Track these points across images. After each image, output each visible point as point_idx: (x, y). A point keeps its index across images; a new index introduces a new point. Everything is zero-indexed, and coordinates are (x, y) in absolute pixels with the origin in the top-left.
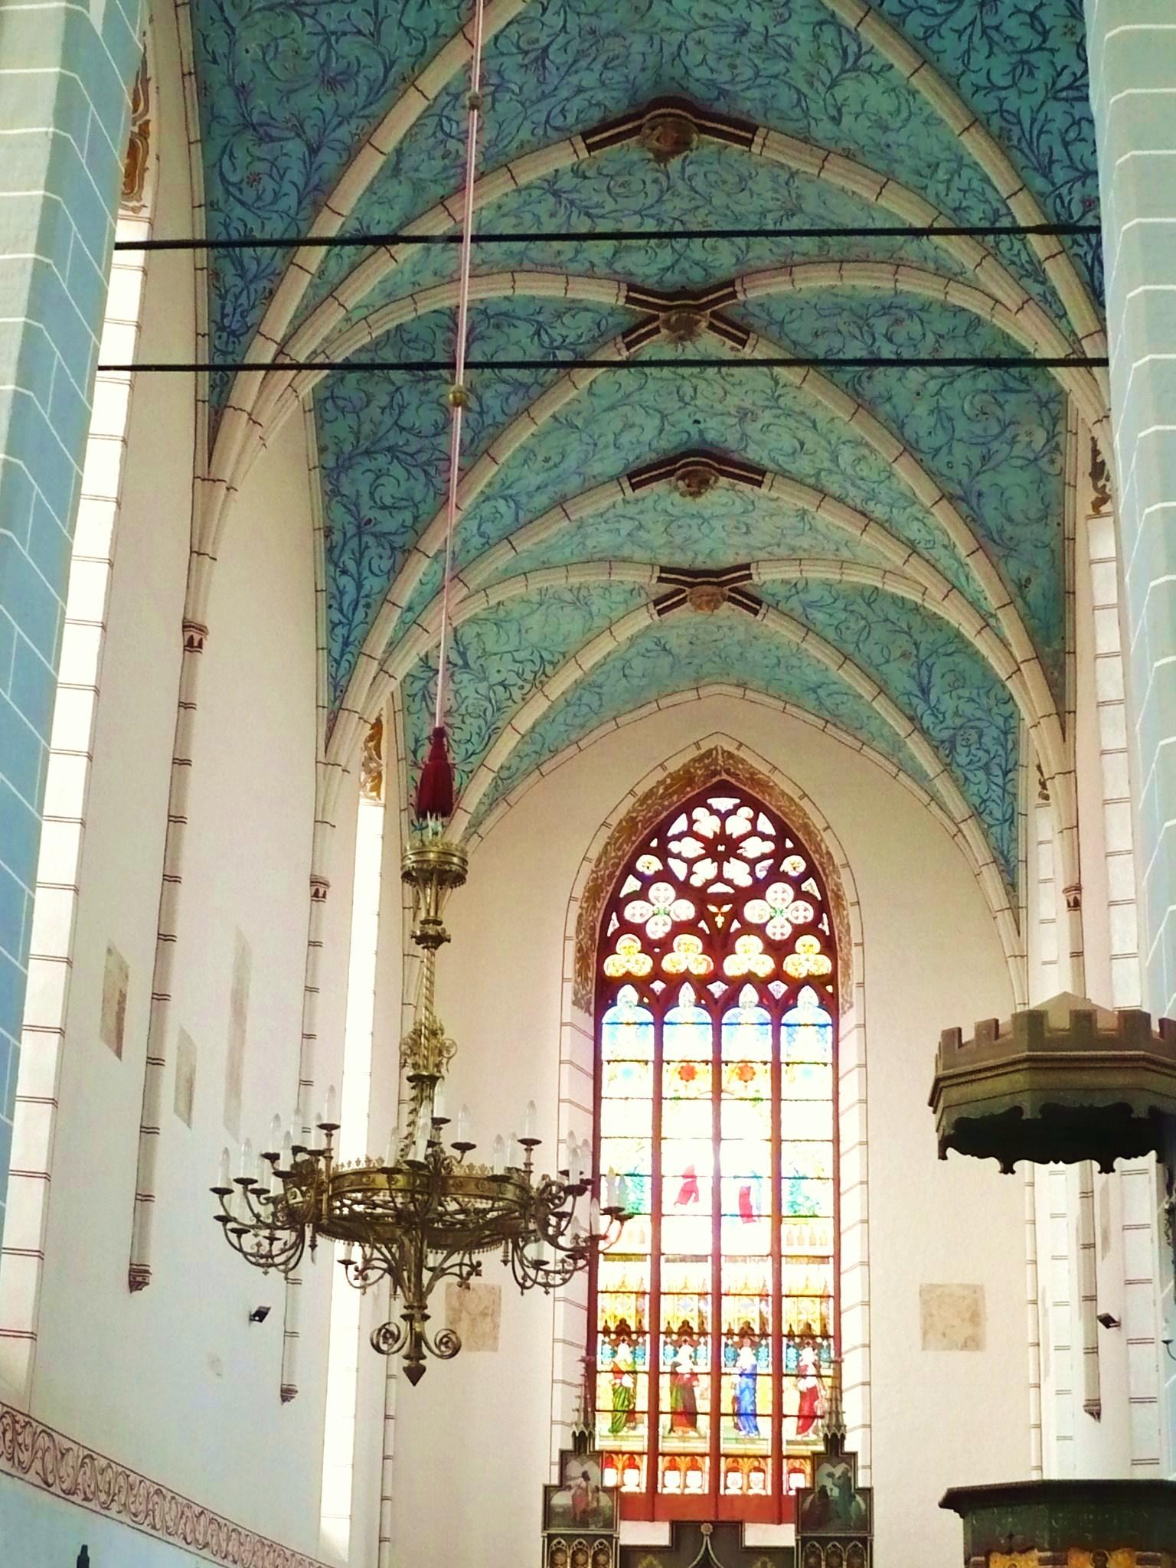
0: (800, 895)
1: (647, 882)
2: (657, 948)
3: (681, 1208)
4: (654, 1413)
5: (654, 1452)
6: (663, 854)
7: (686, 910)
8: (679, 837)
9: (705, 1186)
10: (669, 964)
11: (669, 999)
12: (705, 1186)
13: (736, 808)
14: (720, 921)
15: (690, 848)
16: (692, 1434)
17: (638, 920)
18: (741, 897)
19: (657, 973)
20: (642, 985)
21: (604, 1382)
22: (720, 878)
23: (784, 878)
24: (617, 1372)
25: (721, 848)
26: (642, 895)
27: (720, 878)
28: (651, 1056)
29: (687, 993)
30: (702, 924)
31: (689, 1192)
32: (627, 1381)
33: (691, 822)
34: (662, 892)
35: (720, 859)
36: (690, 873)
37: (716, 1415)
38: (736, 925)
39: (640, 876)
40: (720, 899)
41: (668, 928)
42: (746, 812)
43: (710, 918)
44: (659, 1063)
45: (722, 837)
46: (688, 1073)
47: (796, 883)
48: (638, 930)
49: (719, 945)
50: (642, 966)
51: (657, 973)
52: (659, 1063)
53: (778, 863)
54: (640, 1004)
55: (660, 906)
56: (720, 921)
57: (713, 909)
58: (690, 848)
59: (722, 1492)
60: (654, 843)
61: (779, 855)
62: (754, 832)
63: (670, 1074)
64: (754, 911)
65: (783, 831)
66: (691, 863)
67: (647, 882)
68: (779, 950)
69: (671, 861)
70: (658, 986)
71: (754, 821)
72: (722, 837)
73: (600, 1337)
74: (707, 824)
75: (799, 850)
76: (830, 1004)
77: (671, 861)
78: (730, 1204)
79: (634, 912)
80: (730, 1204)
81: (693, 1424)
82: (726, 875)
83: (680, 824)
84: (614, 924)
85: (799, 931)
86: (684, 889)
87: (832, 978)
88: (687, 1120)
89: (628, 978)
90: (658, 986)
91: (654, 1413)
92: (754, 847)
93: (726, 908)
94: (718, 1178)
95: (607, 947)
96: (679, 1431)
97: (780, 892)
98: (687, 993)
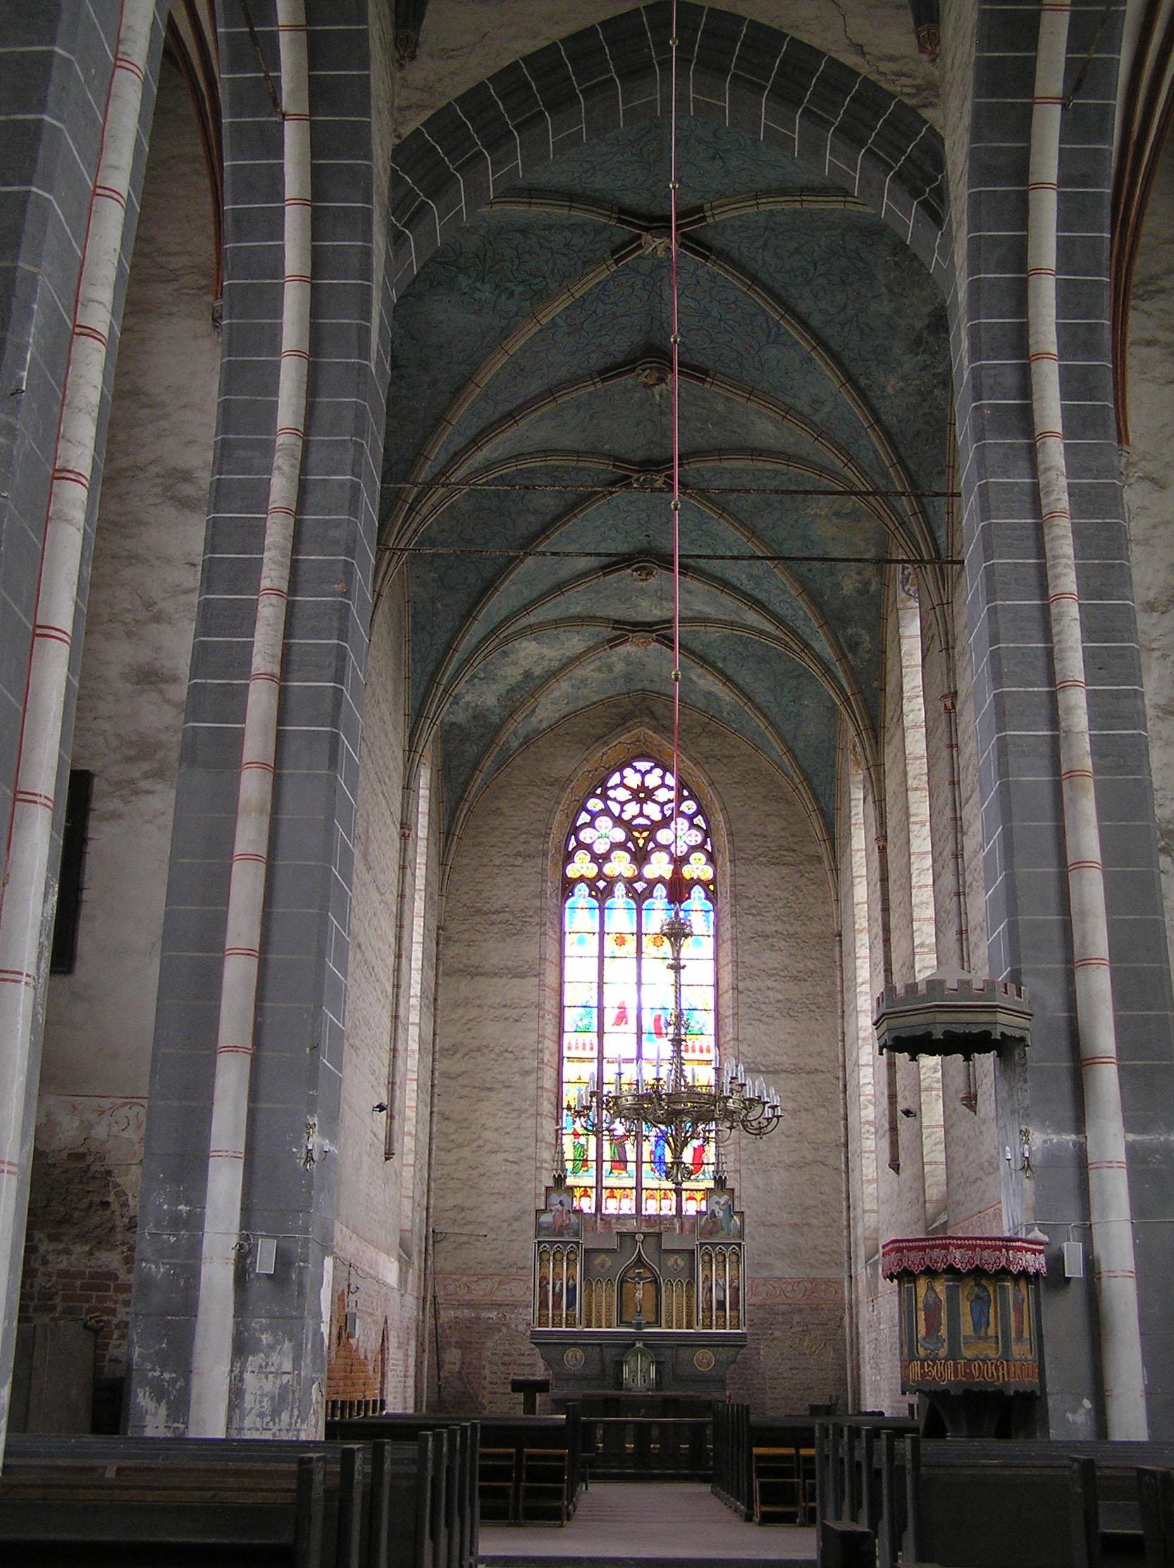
0: (693, 826)
1: (594, 816)
2: (600, 859)
3: (617, 1028)
4: (599, 1160)
5: (599, 1186)
6: (605, 797)
7: (619, 835)
8: (614, 787)
9: (632, 1014)
10: (609, 869)
11: (608, 892)
12: (632, 1014)
13: (652, 768)
14: (641, 842)
15: (623, 795)
16: (624, 1174)
17: (588, 841)
18: (654, 827)
19: (600, 875)
20: (591, 884)
21: (568, 1141)
22: (641, 814)
23: (682, 814)
24: (576, 1135)
25: (643, 795)
26: (591, 824)
27: (641, 814)
28: (597, 929)
29: (620, 889)
30: (630, 844)
31: (621, 1018)
32: (582, 1140)
33: (623, 777)
34: (604, 822)
35: (641, 802)
36: (622, 811)
37: (639, 1162)
38: (651, 845)
39: (589, 812)
40: (643, 828)
41: (608, 847)
42: (658, 772)
43: (635, 841)
44: (602, 934)
45: (643, 788)
46: (621, 941)
47: (690, 818)
48: (588, 847)
49: (640, 857)
50: (591, 871)
51: (600, 875)
52: (602, 934)
53: (679, 806)
54: (590, 895)
55: (603, 832)
56: (641, 842)
57: (637, 834)
58: (623, 795)
59: (644, 1212)
60: (599, 791)
61: (680, 799)
62: (663, 785)
63: (609, 941)
64: (663, 836)
65: (682, 785)
66: (622, 804)
67: (594, 816)
68: (679, 862)
69: (609, 803)
70: (601, 884)
71: (663, 778)
72: (643, 788)
73: (565, 1111)
74: (633, 779)
75: (692, 797)
76: (711, 897)
77: (609, 803)
78: (648, 1025)
79: (586, 835)
80: (648, 1025)
81: (625, 1169)
82: (645, 812)
83: (616, 779)
84: (573, 843)
85: (693, 849)
86: (618, 821)
87: (713, 881)
88: (620, 972)
89: (582, 879)
90: (601, 884)
91: (599, 1160)
92: (663, 795)
93: (645, 834)
94: (640, 1009)
95: (569, 858)
96: (616, 1172)
97: (682, 823)
98: (620, 889)
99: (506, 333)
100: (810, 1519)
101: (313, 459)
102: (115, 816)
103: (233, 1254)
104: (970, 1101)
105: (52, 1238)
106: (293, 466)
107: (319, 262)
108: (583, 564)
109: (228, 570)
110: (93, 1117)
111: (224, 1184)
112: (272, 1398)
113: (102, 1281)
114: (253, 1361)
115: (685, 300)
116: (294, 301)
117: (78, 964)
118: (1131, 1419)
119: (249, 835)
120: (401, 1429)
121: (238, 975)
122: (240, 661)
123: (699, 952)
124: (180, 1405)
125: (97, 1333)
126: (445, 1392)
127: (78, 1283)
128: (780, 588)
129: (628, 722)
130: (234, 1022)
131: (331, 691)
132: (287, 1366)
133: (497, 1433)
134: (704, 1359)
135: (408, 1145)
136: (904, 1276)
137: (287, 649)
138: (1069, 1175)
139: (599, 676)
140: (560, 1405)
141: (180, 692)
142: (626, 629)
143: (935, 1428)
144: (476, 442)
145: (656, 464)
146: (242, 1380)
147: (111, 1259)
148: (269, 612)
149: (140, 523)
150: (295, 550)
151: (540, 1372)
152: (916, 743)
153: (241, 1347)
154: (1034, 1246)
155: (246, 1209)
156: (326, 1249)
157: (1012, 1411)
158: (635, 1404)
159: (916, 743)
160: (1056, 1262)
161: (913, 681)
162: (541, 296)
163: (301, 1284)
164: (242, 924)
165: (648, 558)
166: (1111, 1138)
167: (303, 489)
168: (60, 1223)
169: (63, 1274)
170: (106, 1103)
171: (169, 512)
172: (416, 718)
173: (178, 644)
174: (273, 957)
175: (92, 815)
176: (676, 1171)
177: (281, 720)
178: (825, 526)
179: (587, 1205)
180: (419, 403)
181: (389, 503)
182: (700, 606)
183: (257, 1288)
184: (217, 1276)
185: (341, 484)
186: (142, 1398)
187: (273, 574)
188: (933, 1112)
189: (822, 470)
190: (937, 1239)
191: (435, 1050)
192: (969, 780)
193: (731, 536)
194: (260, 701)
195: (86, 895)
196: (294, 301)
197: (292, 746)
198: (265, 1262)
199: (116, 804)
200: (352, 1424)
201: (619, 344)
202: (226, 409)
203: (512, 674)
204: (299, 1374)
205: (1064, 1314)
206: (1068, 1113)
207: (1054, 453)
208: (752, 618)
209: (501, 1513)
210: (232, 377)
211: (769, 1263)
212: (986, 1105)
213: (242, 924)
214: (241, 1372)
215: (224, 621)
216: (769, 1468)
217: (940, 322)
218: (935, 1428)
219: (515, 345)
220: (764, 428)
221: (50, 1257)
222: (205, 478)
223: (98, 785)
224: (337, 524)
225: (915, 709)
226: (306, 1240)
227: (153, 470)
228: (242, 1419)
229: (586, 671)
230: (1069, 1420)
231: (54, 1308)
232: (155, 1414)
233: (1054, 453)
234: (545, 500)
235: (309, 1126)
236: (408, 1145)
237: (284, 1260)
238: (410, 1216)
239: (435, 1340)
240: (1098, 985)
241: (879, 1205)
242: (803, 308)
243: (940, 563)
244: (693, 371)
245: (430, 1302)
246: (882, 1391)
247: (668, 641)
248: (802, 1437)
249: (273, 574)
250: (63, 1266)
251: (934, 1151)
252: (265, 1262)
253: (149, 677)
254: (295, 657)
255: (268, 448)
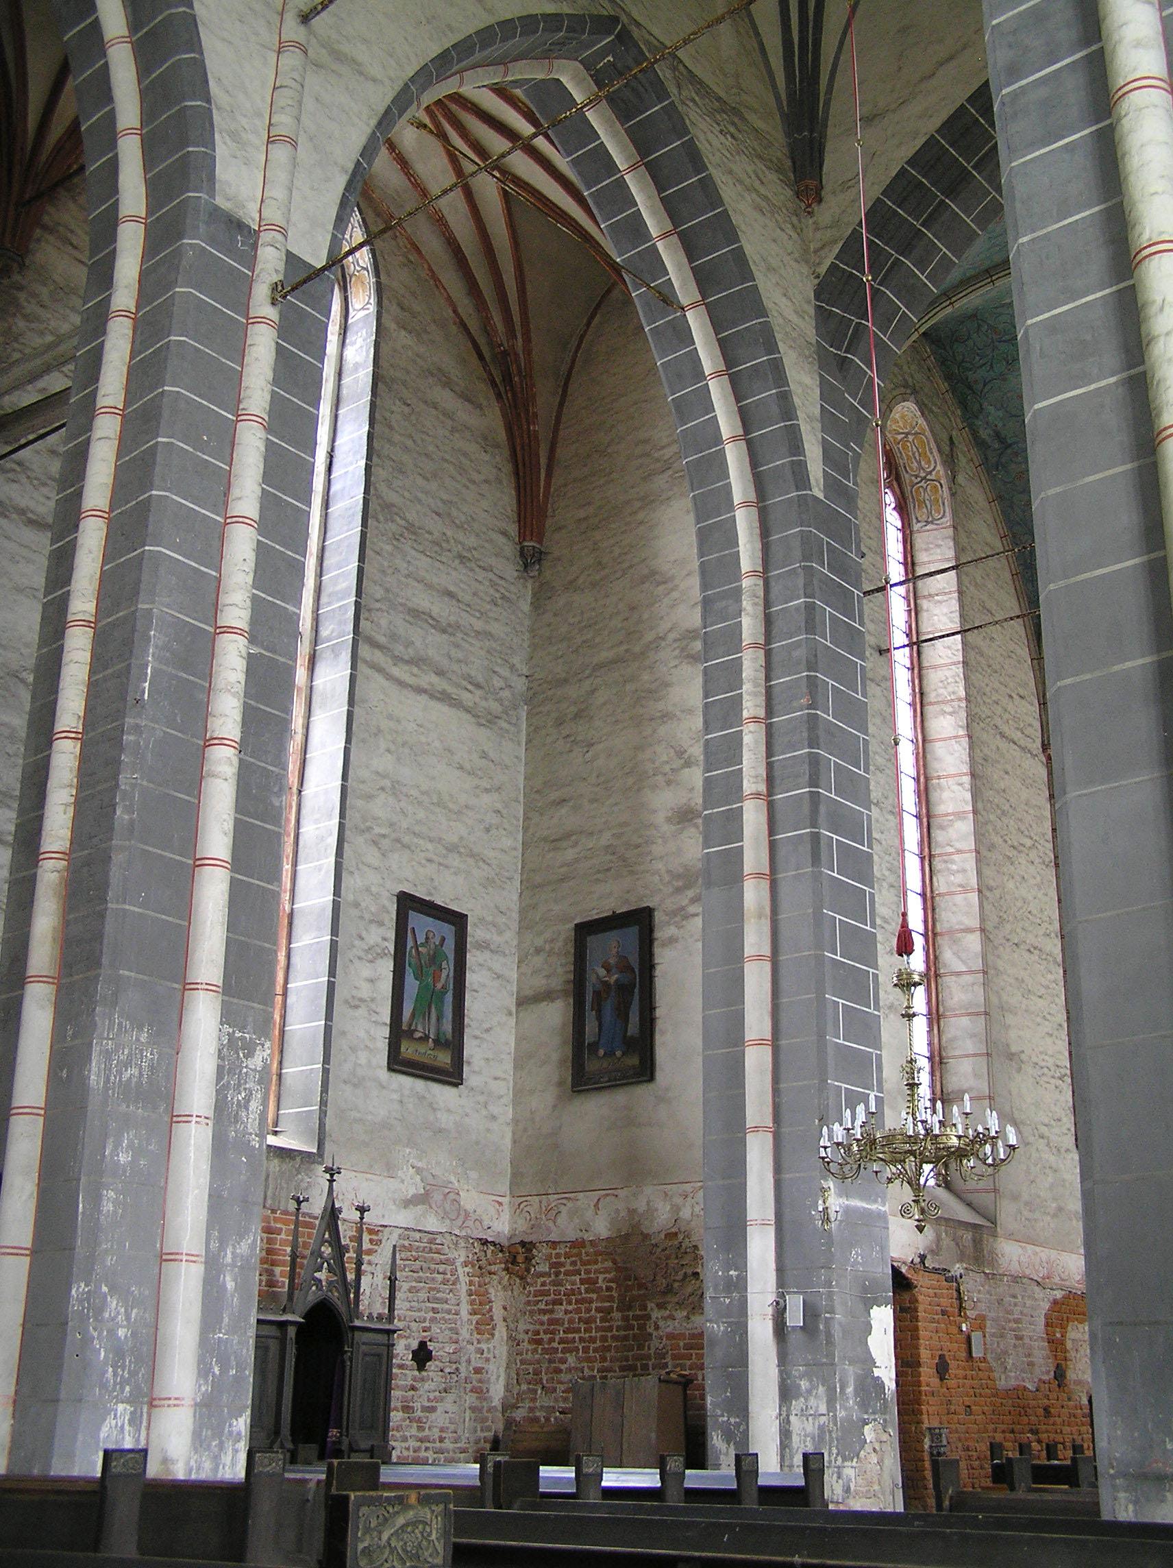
101: (776, 589)
102: (672, 940)
103: (770, 1311)
105: (661, 1306)
106: (756, 604)
110: (678, 1200)
111: (761, 1248)
112: (813, 1438)
114: (797, 1405)
117: (659, 1075)
119: (755, 939)
121: (757, 1062)
127: (681, 1344)
130: (757, 1108)
131: (807, 796)
132: (823, 1409)
137: (770, 766)
146: (789, 1422)
149: (667, 685)
150: (768, 678)
153: (787, 1393)
155: (780, 1270)
163: (829, 1335)
167: (768, 620)
168: (664, 1293)
169: (671, 1336)
170: (687, 1187)
174: (783, 1042)
175: (656, 943)
177: (772, 831)
183: (794, 1339)
184: (761, 1330)
185: (797, 608)
195: (658, 1013)
197: (782, 852)
199: (671, 931)
204: (835, 1416)
210: (704, 537)
214: (788, 1416)
221: (661, 1323)
223: (659, 917)
224: (797, 645)
226: (830, 1295)
227: (671, 636)
228: (792, 1458)
231: (666, 1365)
232: (727, 1454)
235: (823, 1190)
237: (811, 1312)
250: (669, 1330)
254: (777, 773)
255: (737, 594)
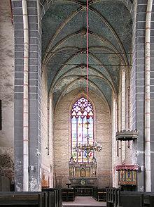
25: (83, 103)
49: (83, 112)
74: (81, 101)
88: (80, 129)
99: (60, 25)
100: (105, 201)
101: (31, 48)
104: (129, 147)
107: (28, 11)
108: (73, 66)
109: (19, 68)
111: (26, 158)
113: (10, 172)
115: (89, 18)
116: (25, 18)
118: (149, 189)
119: (25, 109)
120: (51, 190)
121: (25, 130)
122: (22, 82)
123: (91, 126)
124: (22, 188)
125: (10, 179)
126: (57, 186)
128: (103, 70)
129: (81, 91)
133: (64, 190)
134: (91, 181)
135: (51, 153)
136: (118, 170)
138: (142, 157)
139: (75, 85)
140: (72, 187)
141: (13, 87)
142: (81, 77)
143: (122, 190)
144: (56, 45)
145: (84, 49)
147: (11, 169)
148: (26, 74)
151: (70, 183)
152: (123, 95)
153: (29, 180)
154: (137, 167)
156: (40, 167)
157: (133, 188)
158: (83, 186)
159: (123, 95)
160: (140, 169)
161: (123, 85)
162: (66, 18)
164: (26, 123)
165: (83, 65)
166: (148, 152)
171: (8, 57)
172: (49, 91)
173: (12, 80)
176: (88, 157)
178: (111, 60)
179: (76, 161)
180: (47, 37)
181: (43, 56)
182: (91, 73)
183: (31, 173)
184: (26, 170)
186: (17, 187)
187: (26, 68)
188: (123, 148)
189: (111, 50)
190: (123, 165)
191: (54, 140)
192: (131, 100)
193: (97, 62)
194: (25, 89)
196: (25, 18)
198: (32, 169)
200: (45, 189)
201: (79, 27)
202: (16, 39)
203: (63, 84)
205: (140, 176)
206: (142, 149)
207: (148, 46)
208: (99, 75)
209: (65, 200)
211: (100, 168)
212: (131, 147)
213: (26, 123)
215: (19, 76)
216: (100, 195)
217: (131, 22)
218: (122, 190)
219: (62, 27)
220: (102, 43)
222: (13, 51)
225: (123, 90)
229: (74, 84)
230: (140, 189)
233: (148, 46)
234: (67, 55)
236: (51, 153)
237: (35, 168)
238: (52, 163)
239: (55, 179)
240: (148, 131)
241: (116, 162)
242: (109, 20)
243: (129, 65)
244: (90, 32)
245: (55, 174)
246: (115, 185)
247: (86, 79)
248: (104, 191)
249: (26, 68)
251: (123, 154)
252: (32, 169)
253: (8, 85)
